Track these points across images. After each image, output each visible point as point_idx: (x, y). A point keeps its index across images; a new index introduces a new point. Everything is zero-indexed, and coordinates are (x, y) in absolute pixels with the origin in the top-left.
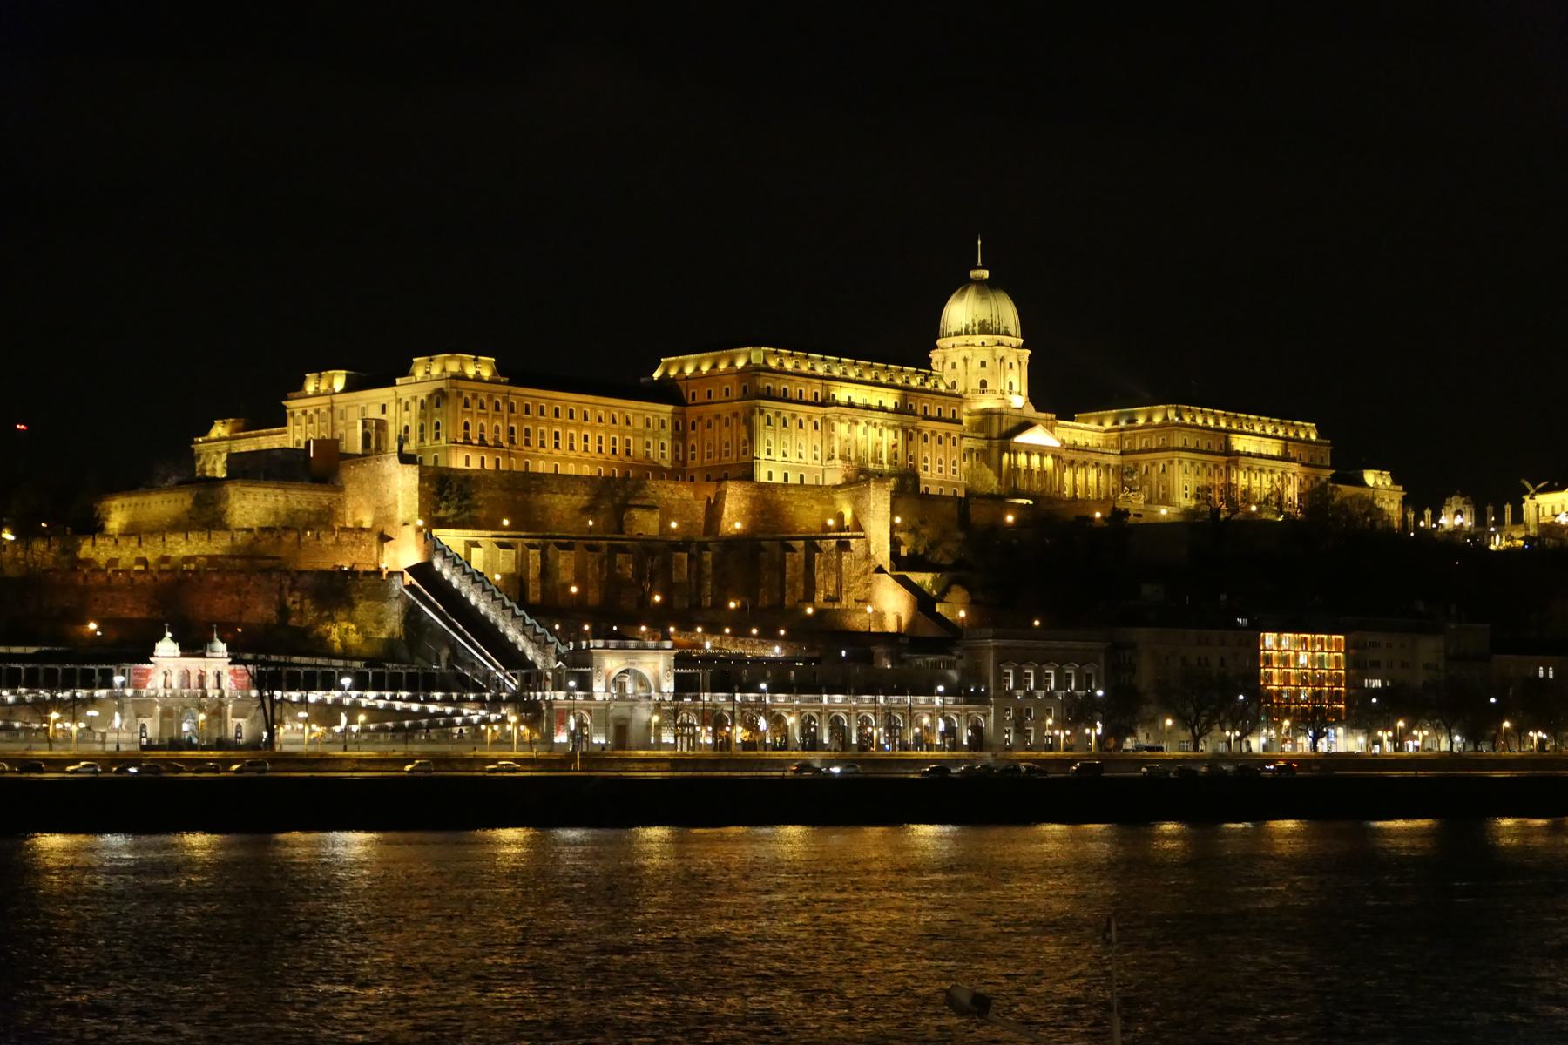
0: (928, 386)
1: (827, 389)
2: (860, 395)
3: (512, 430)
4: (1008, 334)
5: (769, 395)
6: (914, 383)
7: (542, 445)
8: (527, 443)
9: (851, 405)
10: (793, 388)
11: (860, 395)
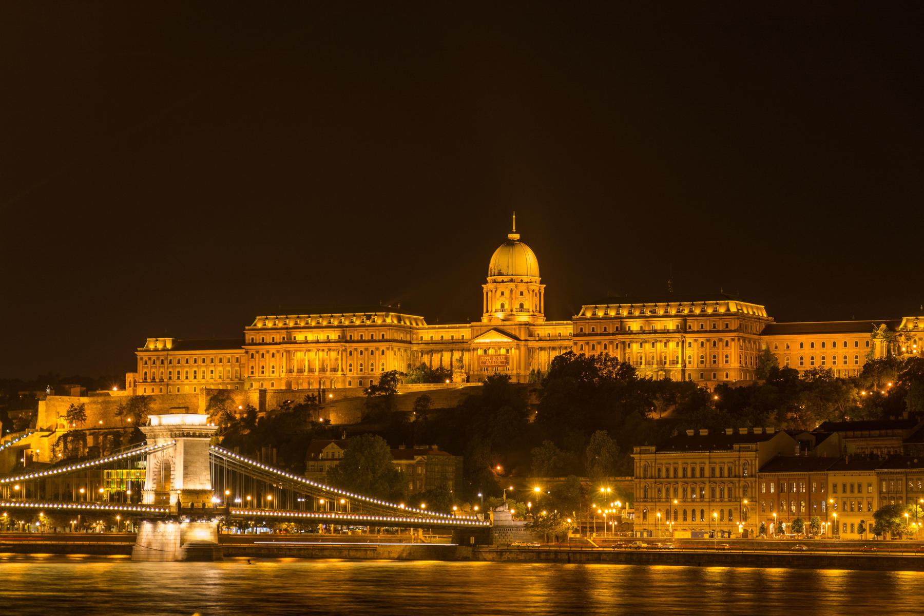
0: (368, 323)
1: (289, 334)
2: (311, 336)
3: (170, 373)
4: (500, 274)
5: (253, 343)
6: (358, 323)
7: (187, 378)
8: (178, 378)
9: (306, 342)
10: (268, 339)
11: (311, 336)
